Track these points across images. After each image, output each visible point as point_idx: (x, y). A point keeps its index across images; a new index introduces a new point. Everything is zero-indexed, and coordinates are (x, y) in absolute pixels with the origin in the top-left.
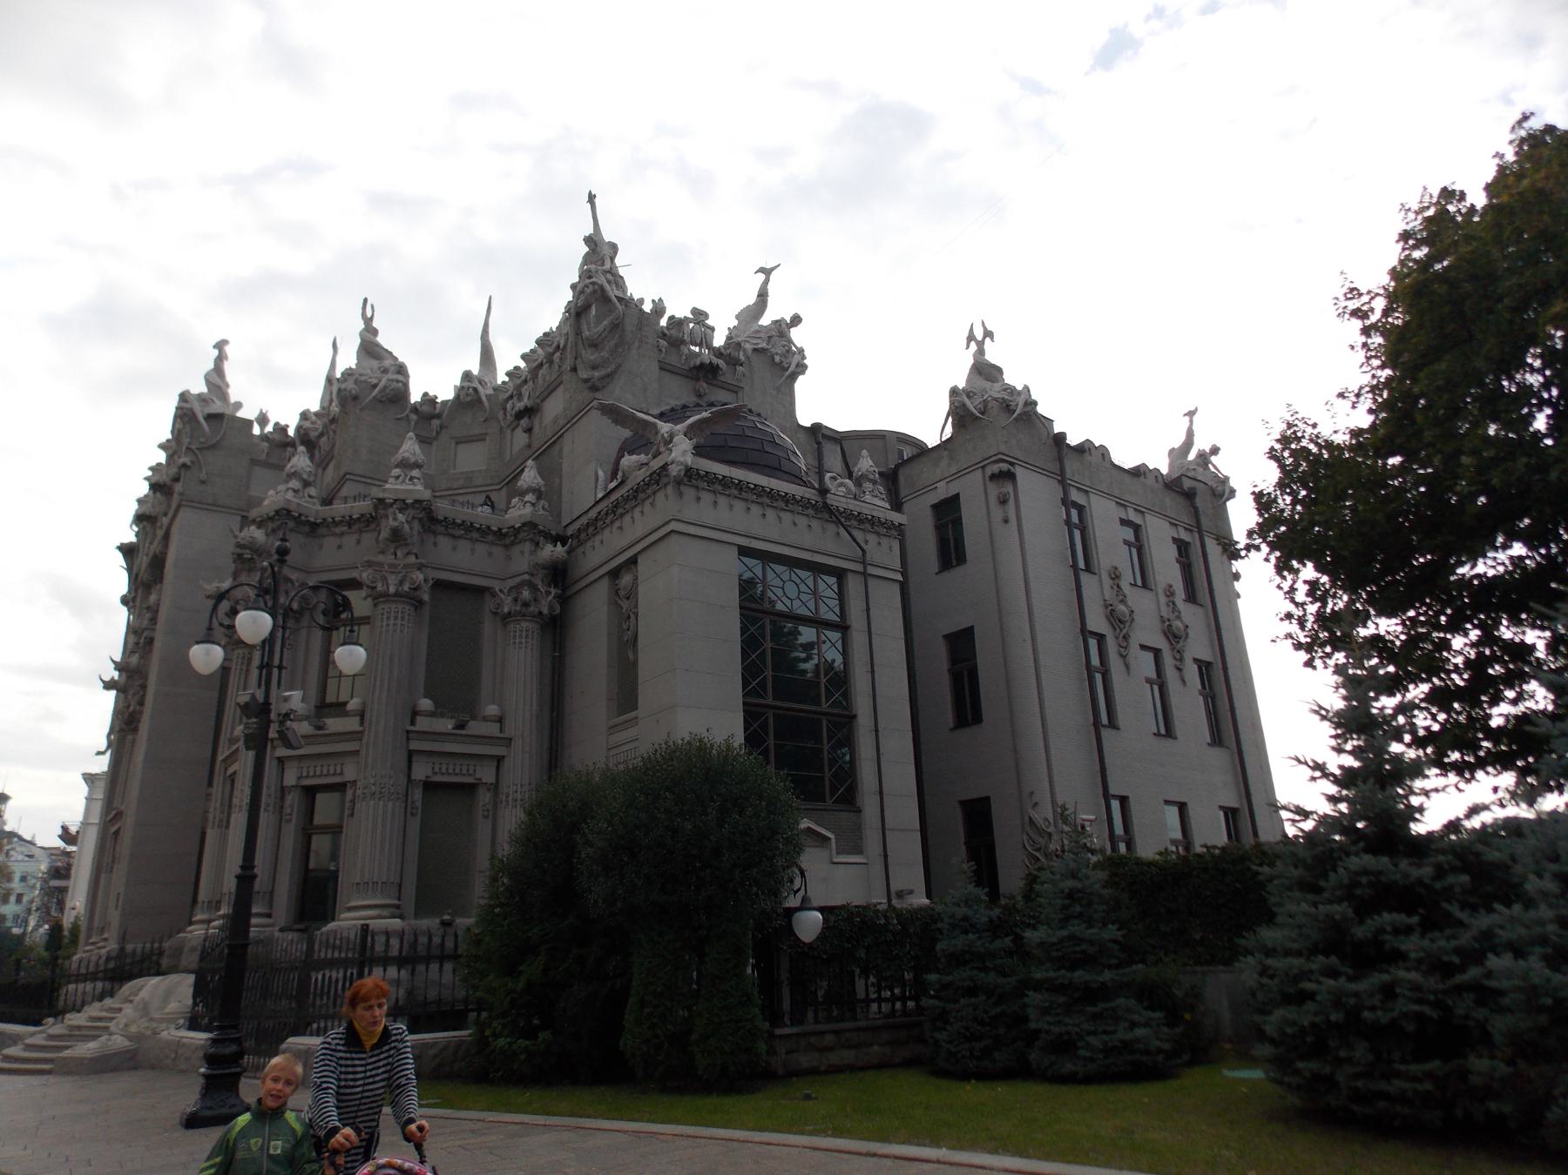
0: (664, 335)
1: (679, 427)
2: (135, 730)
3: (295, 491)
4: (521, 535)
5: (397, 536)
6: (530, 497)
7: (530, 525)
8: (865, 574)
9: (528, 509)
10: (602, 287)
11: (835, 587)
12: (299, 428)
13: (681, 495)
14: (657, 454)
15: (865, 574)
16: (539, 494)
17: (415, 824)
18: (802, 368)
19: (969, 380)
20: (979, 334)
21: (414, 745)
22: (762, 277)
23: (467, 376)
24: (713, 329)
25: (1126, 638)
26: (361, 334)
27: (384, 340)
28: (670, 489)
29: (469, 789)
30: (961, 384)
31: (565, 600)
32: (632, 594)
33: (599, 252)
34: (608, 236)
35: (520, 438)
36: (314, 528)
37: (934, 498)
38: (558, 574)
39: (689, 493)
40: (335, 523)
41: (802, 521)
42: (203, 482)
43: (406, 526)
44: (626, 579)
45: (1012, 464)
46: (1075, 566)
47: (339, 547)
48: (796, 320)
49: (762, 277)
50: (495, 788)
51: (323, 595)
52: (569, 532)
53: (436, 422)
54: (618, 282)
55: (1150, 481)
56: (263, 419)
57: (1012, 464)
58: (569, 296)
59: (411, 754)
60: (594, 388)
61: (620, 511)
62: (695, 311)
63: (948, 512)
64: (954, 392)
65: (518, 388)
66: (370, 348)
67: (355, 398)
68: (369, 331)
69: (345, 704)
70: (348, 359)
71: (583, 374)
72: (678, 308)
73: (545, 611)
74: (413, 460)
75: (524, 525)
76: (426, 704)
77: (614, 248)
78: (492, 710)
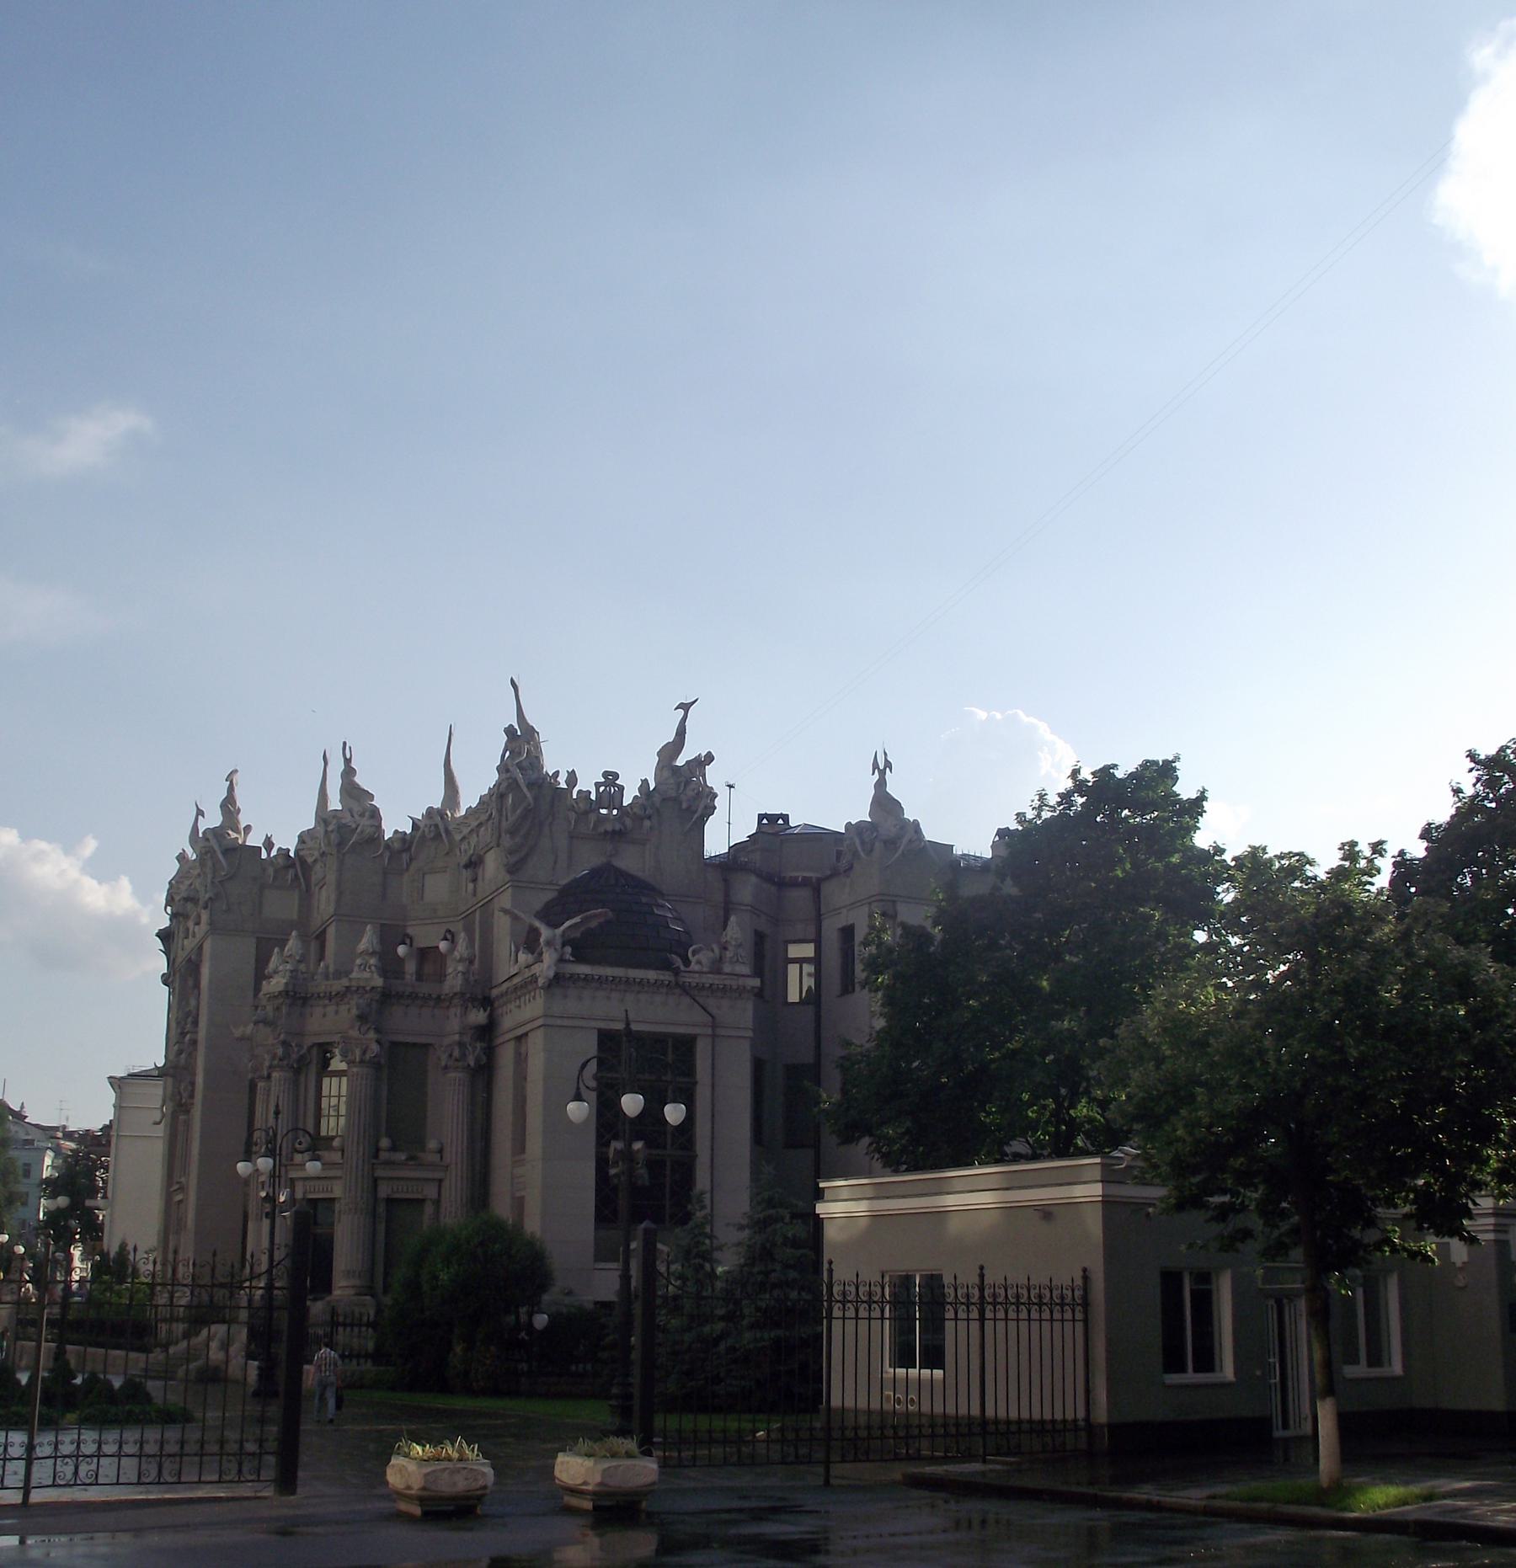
2: (188, 1112)
4: (456, 1001)
8: (714, 1036)
10: (515, 780)
17: (381, 1228)
22: (681, 712)
24: (622, 788)
29: (422, 1201)
31: (490, 1052)
34: (531, 720)
37: (842, 921)
38: (487, 1032)
48: (710, 758)
49: (681, 712)
50: (437, 1203)
51: (315, 1051)
56: (269, 844)
62: (606, 774)
68: (349, 772)
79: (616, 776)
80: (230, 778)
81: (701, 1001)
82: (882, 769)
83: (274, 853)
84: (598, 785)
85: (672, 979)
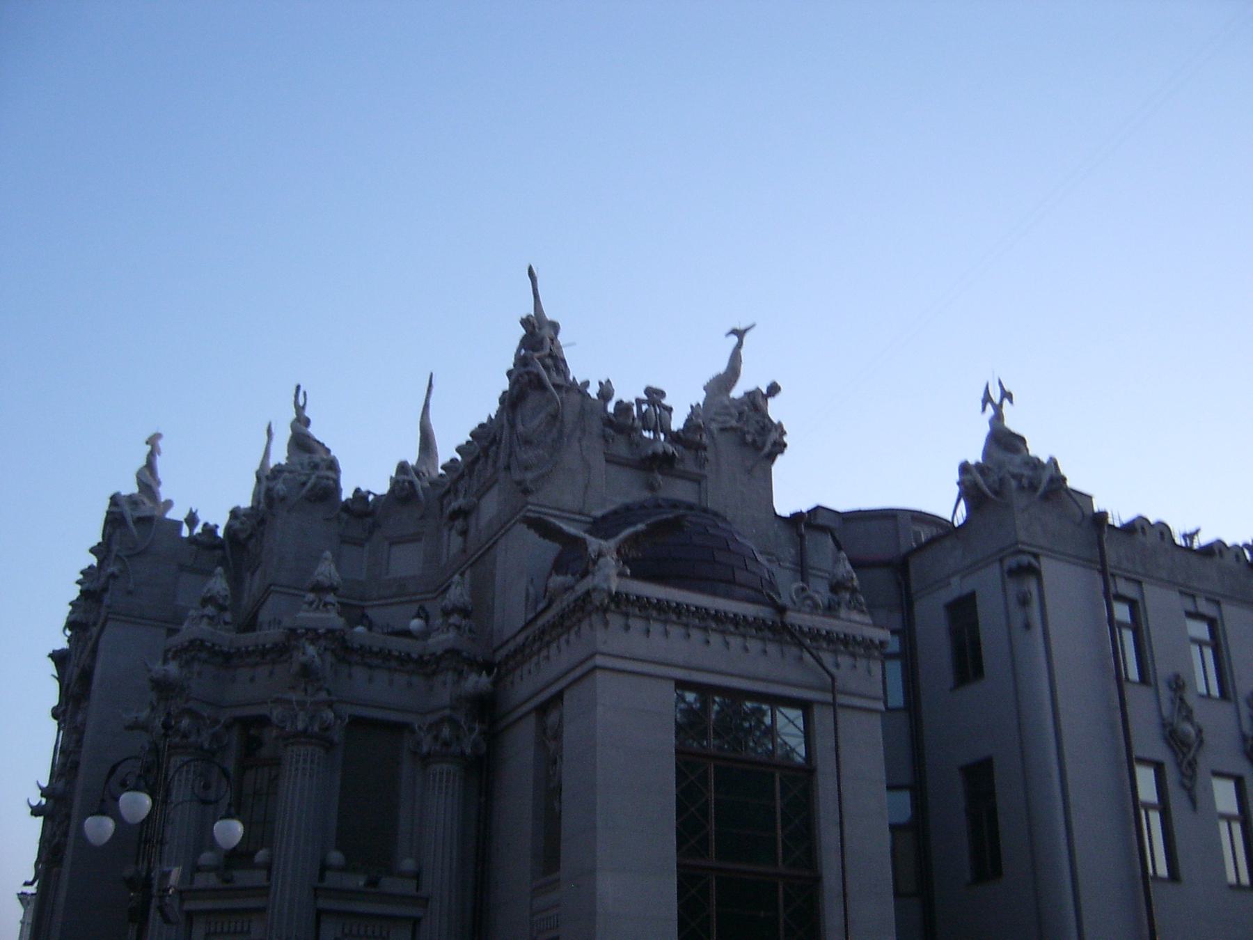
0: (609, 422)
1: (610, 545)
3: (211, 618)
5: (307, 672)
6: (454, 619)
7: (453, 652)
9: (452, 634)
10: (538, 377)
11: (800, 723)
12: (228, 528)
13: (606, 624)
14: (585, 574)
15: (834, 705)
16: (465, 612)
18: (780, 447)
19: (986, 453)
20: (996, 395)
21: (323, 904)
22: (734, 339)
23: (403, 467)
24: (670, 410)
25: (1192, 765)
26: (293, 426)
27: (316, 431)
28: (594, 617)
30: (975, 455)
31: (493, 736)
32: (558, 737)
33: (538, 339)
34: (550, 315)
35: (456, 542)
36: (227, 659)
38: (486, 709)
39: (615, 620)
40: (249, 653)
41: (754, 645)
42: (130, 593)
43: (317, 660)
44: (553, 718)
45: (1036, 556)
46: (1120, 679)
47: (252, 680)
48: (774, 389)
52: (499, 656)
53: (370, 520)
54: (557, 363)
55: (1229, 559)
56: (192, 519)
57: (1036, 556)
58: (505, 384)
59: (319, 913)
60: (526, 492)
61: (547, 638)
62: (649, 391)
63: (963, 611)
64: (964, 468)
65: (455, 483)
66: (302, 442)
67: (283, 499)
68: (301, 421)
69: (253, 854)
70: (280, 456)
71: (517, 475)
72: (628, 391)
73: (468, 751)
74: (327, 583)
75: (447, 651)
76: (336, 857)
77: (555, 327)
78: (408, 864)
79: (662, 394)
80: (153, 441)
81: (814, 652)
82: (996, 401)
83: (198, 529)
84: (639, 402)
85: (778, 619)
